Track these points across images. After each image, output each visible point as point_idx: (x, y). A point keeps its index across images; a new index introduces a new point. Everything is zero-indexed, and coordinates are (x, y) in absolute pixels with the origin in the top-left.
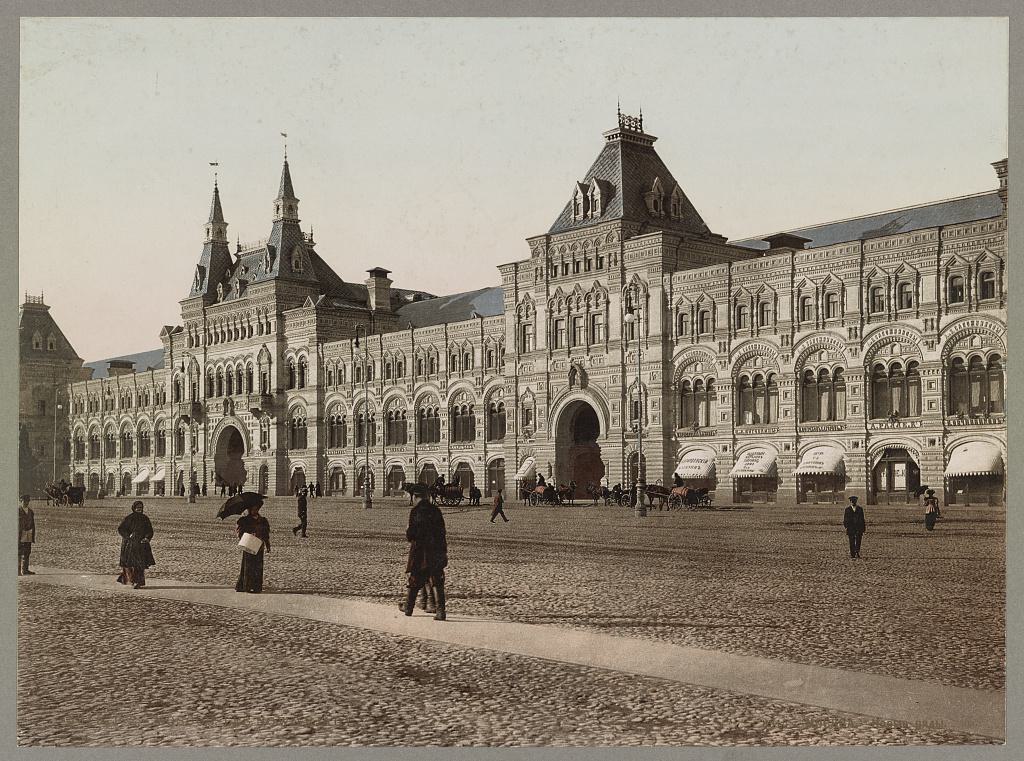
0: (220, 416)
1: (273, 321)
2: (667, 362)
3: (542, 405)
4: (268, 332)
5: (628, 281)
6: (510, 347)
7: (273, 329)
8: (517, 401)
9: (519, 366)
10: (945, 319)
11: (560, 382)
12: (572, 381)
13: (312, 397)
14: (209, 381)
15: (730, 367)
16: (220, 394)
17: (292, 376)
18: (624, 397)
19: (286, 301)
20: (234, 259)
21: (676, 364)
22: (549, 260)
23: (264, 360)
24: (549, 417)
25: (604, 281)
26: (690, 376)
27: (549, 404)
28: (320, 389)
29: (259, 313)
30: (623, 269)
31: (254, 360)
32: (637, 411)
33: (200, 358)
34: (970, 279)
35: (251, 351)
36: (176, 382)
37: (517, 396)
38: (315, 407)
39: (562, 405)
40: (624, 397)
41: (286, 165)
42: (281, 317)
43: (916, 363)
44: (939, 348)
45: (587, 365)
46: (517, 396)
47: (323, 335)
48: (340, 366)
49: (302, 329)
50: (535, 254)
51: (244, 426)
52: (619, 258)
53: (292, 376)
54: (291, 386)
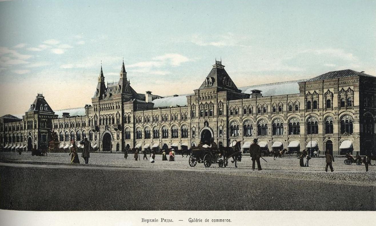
0: (104, 130)
1: (121, 105)
2: (228, 121)
3: (197, 130)
4: (119, 108)
5: (218, 102)
6: (189, 116)
7: (120, 107)
8: (191, 129)
9: (191, 121)
10: (288, 115)
11: (202, 125)
12: (205, 125)
13: (132, 125)
14: (100, 120)
15: (242, 123)
16: (104, 124)
17: (125, 120)
18: (217, 129)
19: (124, 100)
20: (106, 87)
21: (230, 122)
22: (199, 96)
23: (118, 115)
24: (199, 134)
25: (213, 102)
26: (233, 124)
27: (199, 130)
28: (134, 124)
29: (116, 103)
30: (217, 99)
31: (115, 116)
32: (221, 132)
33: (98, 114)
34: (293, 106)
35: (114, 113)
36: (89, 120)
37: (191, 128)
38: (133, 128)
39: (202, 131)
40: (217, 129)
41: (123, 63)
42: (123, 104)
43: (282, 124)
44: (287, 120)
45: (208, 121)
46: (191, 128)
47: (135, 110)
48: (140, 118)
49: (128, 109)
50: (196, 94)
51: (111, 133)
52: (216, 96)
53: (125, 120)
54: (126, 122)
